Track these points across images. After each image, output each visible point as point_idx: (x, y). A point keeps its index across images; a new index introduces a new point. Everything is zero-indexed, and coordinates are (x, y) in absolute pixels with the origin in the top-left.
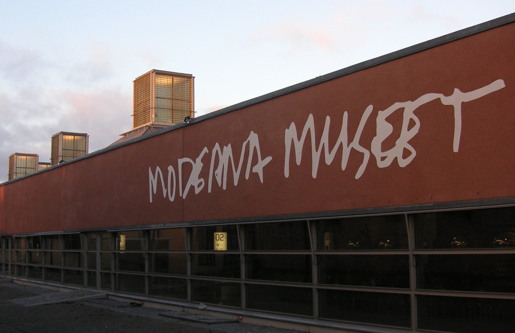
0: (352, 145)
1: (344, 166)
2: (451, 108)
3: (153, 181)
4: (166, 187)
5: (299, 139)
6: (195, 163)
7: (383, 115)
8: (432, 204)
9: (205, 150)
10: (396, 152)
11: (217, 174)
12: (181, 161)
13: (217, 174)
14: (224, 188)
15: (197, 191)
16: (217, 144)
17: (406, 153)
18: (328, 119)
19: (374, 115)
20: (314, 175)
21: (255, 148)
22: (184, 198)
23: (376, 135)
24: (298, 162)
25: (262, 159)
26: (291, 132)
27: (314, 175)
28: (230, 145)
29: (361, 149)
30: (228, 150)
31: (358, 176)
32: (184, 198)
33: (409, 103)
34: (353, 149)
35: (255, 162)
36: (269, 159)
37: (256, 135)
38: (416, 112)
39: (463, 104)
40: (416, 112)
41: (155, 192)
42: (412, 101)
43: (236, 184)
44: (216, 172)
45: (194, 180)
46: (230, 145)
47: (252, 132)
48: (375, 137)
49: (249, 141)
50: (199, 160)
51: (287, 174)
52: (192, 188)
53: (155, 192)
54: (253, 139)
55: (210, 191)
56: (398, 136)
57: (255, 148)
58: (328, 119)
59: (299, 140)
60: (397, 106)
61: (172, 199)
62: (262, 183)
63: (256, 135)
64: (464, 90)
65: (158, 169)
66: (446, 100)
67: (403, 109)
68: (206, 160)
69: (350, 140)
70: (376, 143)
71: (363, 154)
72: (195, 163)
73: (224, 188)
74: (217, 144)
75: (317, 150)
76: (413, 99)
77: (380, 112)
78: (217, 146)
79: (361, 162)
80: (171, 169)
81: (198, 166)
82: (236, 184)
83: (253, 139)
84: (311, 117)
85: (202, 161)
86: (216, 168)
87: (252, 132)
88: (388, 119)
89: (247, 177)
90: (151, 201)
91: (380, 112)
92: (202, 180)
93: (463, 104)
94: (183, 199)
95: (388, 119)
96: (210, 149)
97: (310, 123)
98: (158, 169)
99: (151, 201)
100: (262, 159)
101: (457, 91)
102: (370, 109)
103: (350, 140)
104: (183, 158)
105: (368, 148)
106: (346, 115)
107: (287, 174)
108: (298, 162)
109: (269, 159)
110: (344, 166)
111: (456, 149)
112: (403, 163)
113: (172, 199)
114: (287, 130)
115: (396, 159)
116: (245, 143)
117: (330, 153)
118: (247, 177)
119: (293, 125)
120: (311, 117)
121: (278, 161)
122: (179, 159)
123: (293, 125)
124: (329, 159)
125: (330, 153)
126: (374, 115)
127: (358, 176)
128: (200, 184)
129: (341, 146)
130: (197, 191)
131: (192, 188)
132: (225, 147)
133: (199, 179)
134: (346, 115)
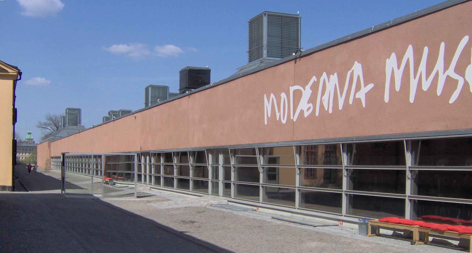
0: (447, 73)
1: (439, 92)
3: (268, 106)
5: (399, 68)
6: (305, 90)
9: (314, 79)
11: (324, 100)
12: (292, 89)
13: (324, 100)
15: (306, 114)
16: (324, 74)
18: (426, 50)
20: (412, 100)
21: (359, 77)
22: (295, 120)
23: (470, 64)
24: (397, 88)
25: (365, 86)
26: (391, 62)
27: (412, 100)
28: (336, 74)
29: (455, 76)
30: (334, 78)
31: (451, 101)
32: (295, 120)
34: (448, 77)
35: (358, 88)
36: (371, 86)
43: (340, 108)
44: (323, 98)
45: (304, 105)
46: (336, 74)
47: (356, 62)
48: (469, 65)
50: (308, 87)
51: (386, 99)
52: (302, 112)
55: (317, 114)
57: (359, 77)
61: (284, 122)
63: (360, 65)
65: (272, 96)
68: (315, 87)
69: (446, 68)
71: (458, 80)
72: (305, 90)
73: (330, 111)
74: (324, 74)
75: (415, 78)
78: (324, 75)
79: (455, 88)
80: (283, 95)
81: (307, 93)
82: (340, 108)
84: (410, 48)
85: (311, 88)
86: (323, 94)
87: (356, 62)
89: (351, 102)
90: (266, 123)
92: (311, 105)
94: (294, 122)
96: (318, 78)
97: (409, 53)
98: (272, 96)
99: (266, 123)
100: (365, 86)
103: (446, 68)
104: (294, 86)
105: (463, 75)
106: (443, 45)
107: (386, 99)
108: (397, 88)
109: (371, 86)
110: (439, 92)
113: (284, 122)
114: (388, 59)
116: (349, 73)
117: (427, 80)
118: (351, 102)
119: (393, 55)
120: (410, 48)
121: (379, 88)
123: (393, 55)
124: (426, 86)
125: (427, 80)
127: (451, 101)
128: (308, 109)
130: (306, 114)
131: (302, 112)
132: (331, 75)
133: (308, 103)
134: (443, 45)
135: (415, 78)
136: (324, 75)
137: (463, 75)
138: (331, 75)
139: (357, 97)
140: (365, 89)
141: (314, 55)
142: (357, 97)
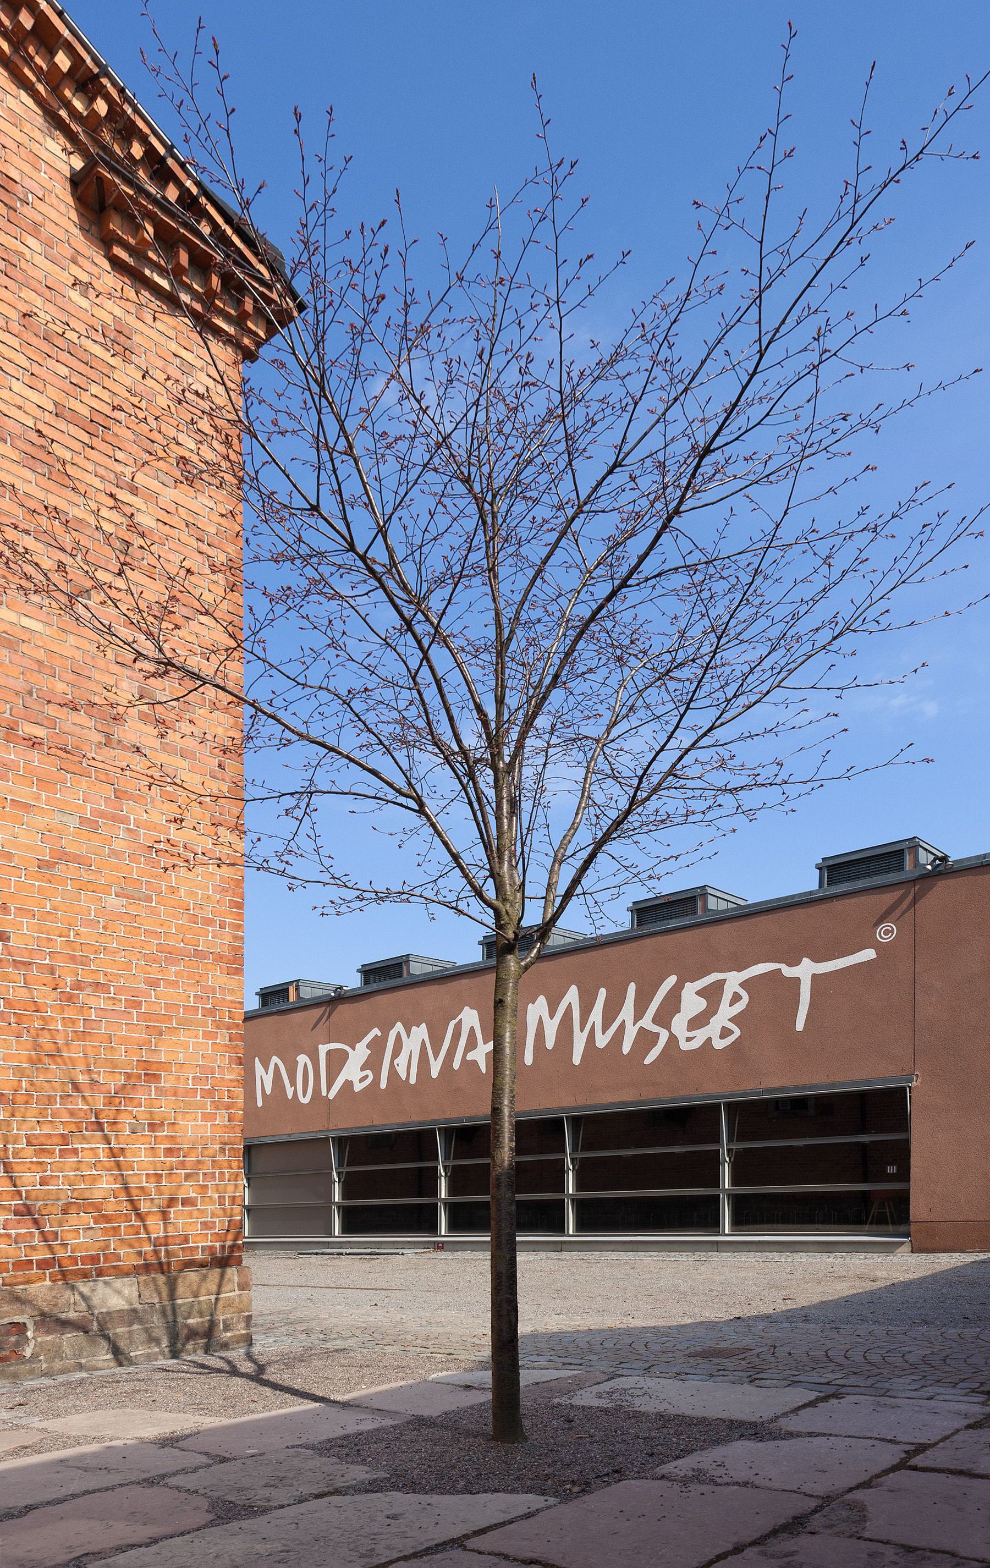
0: (639, 1024)
1: (626, 1048)
2: (796, 981)
9: (376, 1032)
12: (323, 1049)
15: (358, 1087)
17: (725, 1033)
18: (603, 992)
19: (677, 989)
20: (577, 1060)
21: (472, 1029)
24: (550, 1043)
26: (537, 1009)
27: (577, 1060)
28: (424, 1025)
29: (655, 1029)
30: (421, 1033)
31: (648, 1060)
33: (734, 973)
35: (472, 1044)
37: (475, 1012)
39: (814, 976)
41: (268, 1091)
44: (396, 1062)
46: (424, 1025)
52: (348, 1084)
53: (268, 1091)
55: (383, 1085)
56: (715, 1013)
57: (472, 1029)
58: (603, 992)
59: (552, 1017)
60: (715, 977)
62: (484, 1071)
65: (275, 1059)
66: (788, 971)
67: (725, 981)
68: (377, 1047)
69: (638, 1016)
73: (413, 1080)
78: (399, 1027)
79: (655, 1043)
80: (303, 1059)
81: (360, 1053)
86: (396, 1053)
88: (699, 993)
89: (456, 1065)
91: (687, 984)
92: (369, 1072)
93: (814, 976)
95: (699, 993)
97: (572, 996)
98: (275, 1059)
101: (806, 961)
102: (672, 980)
103: (638, 1016)
105: (668, 1027)
106: (632, 988)
108: (550, 1043)
110: (626, 1048)
111: (800, 1025)
112: (719, 1044)
114: (530, 1006)
116: (452, 1024)
118: (456, 1065)
123: (542, 1000)
124: (602, 1041)
126: (677, 989)
127: (648, 1060)
128: (362, 1080)
129: (623, 1025)
130: (358, 1087)
132: (414, 1028)
133: (363, 1069)
134: (632, 988)
136: (399, 1027)
137: (668, 1027)
138: (414, 1028)
139: (468, 1058)
142: (468, 1058)
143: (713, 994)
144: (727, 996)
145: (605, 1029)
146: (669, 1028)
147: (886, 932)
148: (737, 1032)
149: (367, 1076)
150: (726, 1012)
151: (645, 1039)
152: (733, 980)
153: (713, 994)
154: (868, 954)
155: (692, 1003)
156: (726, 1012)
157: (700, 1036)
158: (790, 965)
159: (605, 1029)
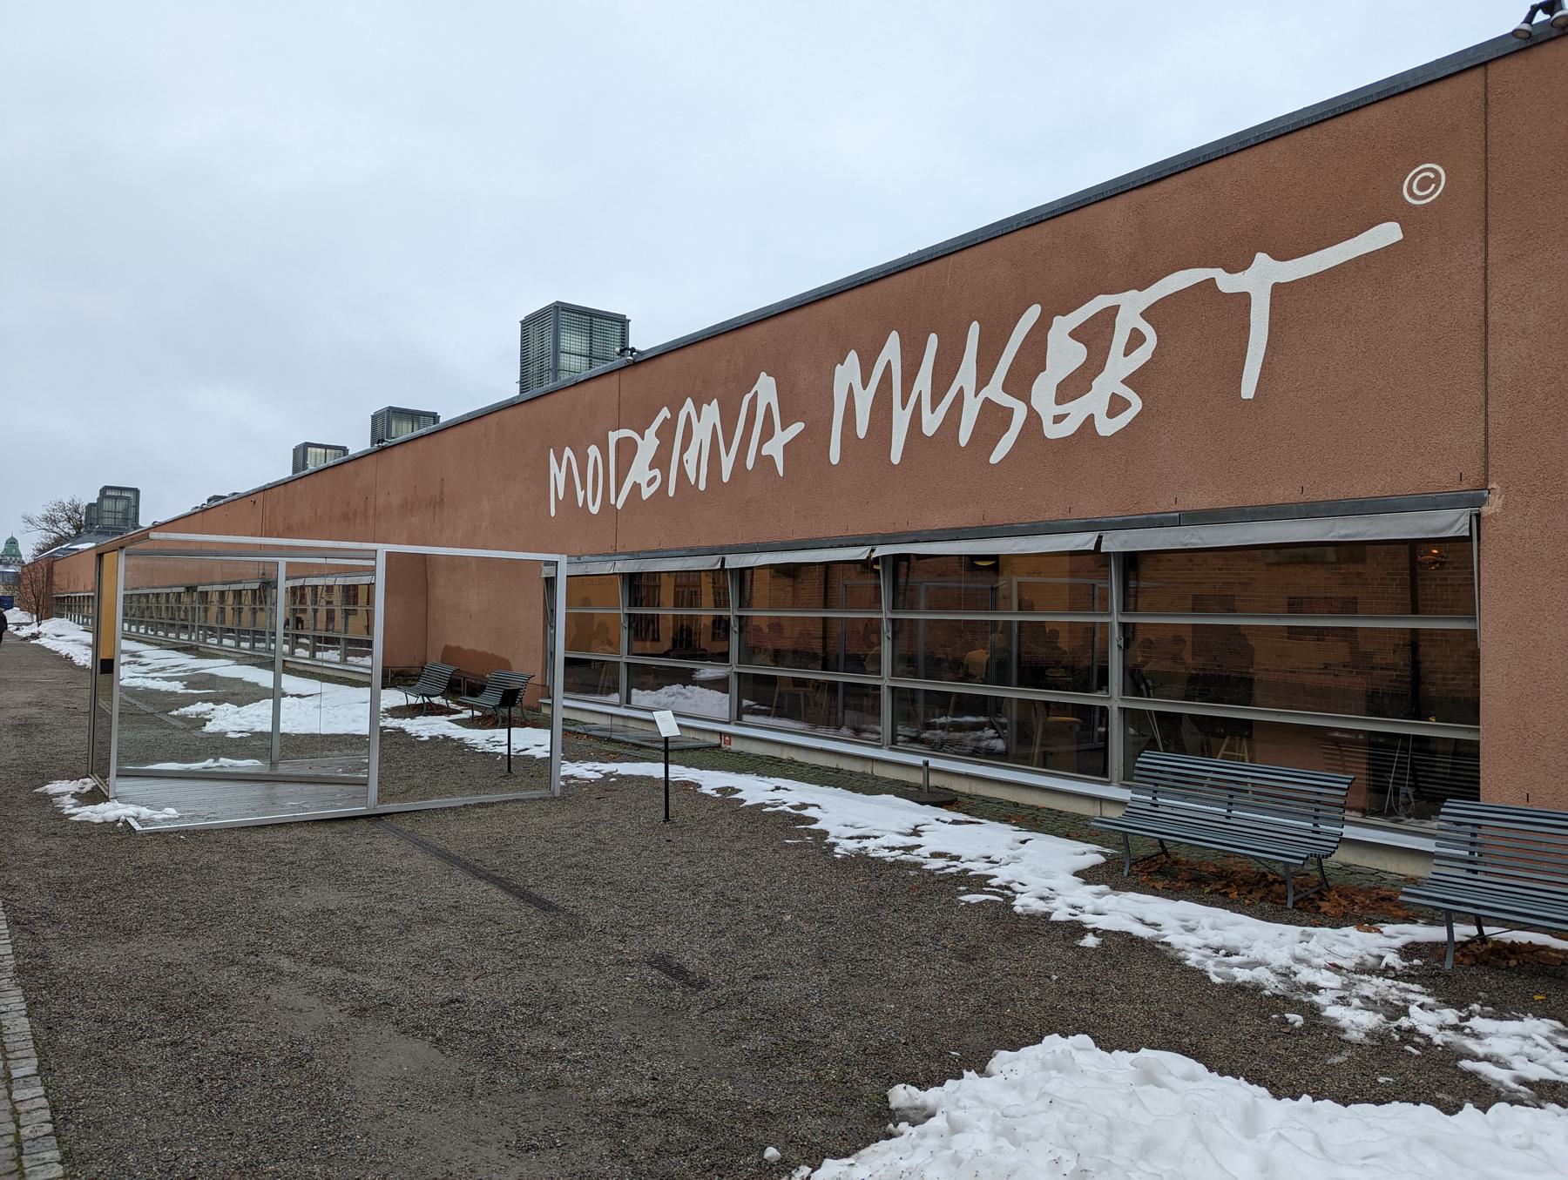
0: (986, 392)
1: (964, 438)
2: (1244, 299)
3: (557, 475)
4: (584, 487)
5: (865, 385)
7: (1063, 325)
8: (1177, 514)
9: (665, 413)
10: (1093, 403)
12: (613, 437)
13: (687, 461)
14: (702, 486)
15: (646, 493)
16: (689, 400)
17: (1117, 405)
18: (933, 339)
19: (1043, 326)
22: (619, 506)
24: (862, 431)
26: (847, 372)
28: (715, 402)
29: (1006, 400)
30: (712, 412)
32: (619, 506)
35: (767, 434)
36: (797, 428)
37: (772, 380)
38: (1146, 315)
39: (1277, 289)
40: (1146, 315)
42: (1140, 289)
43: (726, 478)
44: (685, 457)
45: (641, 472)
46: (715, 402)
47: (763, 374)
49: (756, 392)
50: (650, 433)
51: (835, 457)
52: (636, 487)
53: (561, 496)
54: (766, 389)
55: (671, 493)
56: (1101, 368)
58: (933, 339)
60: (1101, 302)
61: (594, 510)
64: (1281, 255)
65: (568, 452)
66: (1228, 283)
67: (1116, 309)
69: (983, 380)
70: (1044, 390)
71: (1010, 411)
73: (702, 486)
74: (689, 400)
75: (904, 408)
76: (1142, 286)
77: (1057, 319)
79: (1006, 426)
80: (593, 451)
81: (648, 445)
82: (726, 478)
83: (766, 389)
84: (894, 338)
86: (685, 448)
87: (763, 374)
88: (1074, 335)
89: (750, 464)
91: (1057, 319)
92: (657, 472)
93: (1277, 289)
95: (1074, 335)
97: (892, 351)
98: (568, 452)
101: (1261, 258)
102: (1033, 313)
103: (983, 380)
105: (1026, 399)
106: (975, 327)
108: (862, 431)
109: (797, 428)
110: (964, 438)
113: (594, 510)
115: (1091, 418)
116: (747, 398)
118: (750, 464)
119: (853, 357)
120: (894, 338)
122: (610, 432)
123: (853, 357)
124: (931, 423)
126: (1043, 326)
127: (995, 458)
128: (651, 482)
129: (960, 395)
130: (646, 493)
131: (636, 487)
132: (705, 406)
133: (651, 467)
134: (974, 330)
135: (904, 408)
137: (1026, 399)
138: (705, 406)
139: (764, 452)
140: (783, 437)
141: (666, 359)
142: (764, 452)
143: (1096, 335)
144: (1120, 338)
145: (936, 401)
146: (1028, 403)
147: (1424, 184)
148: (1137, 404)
149: (655, 477)
150: (1120, 365)
151: (994, 418)
152: (1131, 306)
153: (1096, 335)
154: (1387, 234)
155: (1065, 354)
156: (1120, 365)
157: (1077, 411)
158: (1231, 270)
159: (936, 401)
